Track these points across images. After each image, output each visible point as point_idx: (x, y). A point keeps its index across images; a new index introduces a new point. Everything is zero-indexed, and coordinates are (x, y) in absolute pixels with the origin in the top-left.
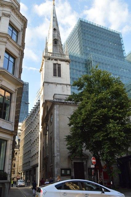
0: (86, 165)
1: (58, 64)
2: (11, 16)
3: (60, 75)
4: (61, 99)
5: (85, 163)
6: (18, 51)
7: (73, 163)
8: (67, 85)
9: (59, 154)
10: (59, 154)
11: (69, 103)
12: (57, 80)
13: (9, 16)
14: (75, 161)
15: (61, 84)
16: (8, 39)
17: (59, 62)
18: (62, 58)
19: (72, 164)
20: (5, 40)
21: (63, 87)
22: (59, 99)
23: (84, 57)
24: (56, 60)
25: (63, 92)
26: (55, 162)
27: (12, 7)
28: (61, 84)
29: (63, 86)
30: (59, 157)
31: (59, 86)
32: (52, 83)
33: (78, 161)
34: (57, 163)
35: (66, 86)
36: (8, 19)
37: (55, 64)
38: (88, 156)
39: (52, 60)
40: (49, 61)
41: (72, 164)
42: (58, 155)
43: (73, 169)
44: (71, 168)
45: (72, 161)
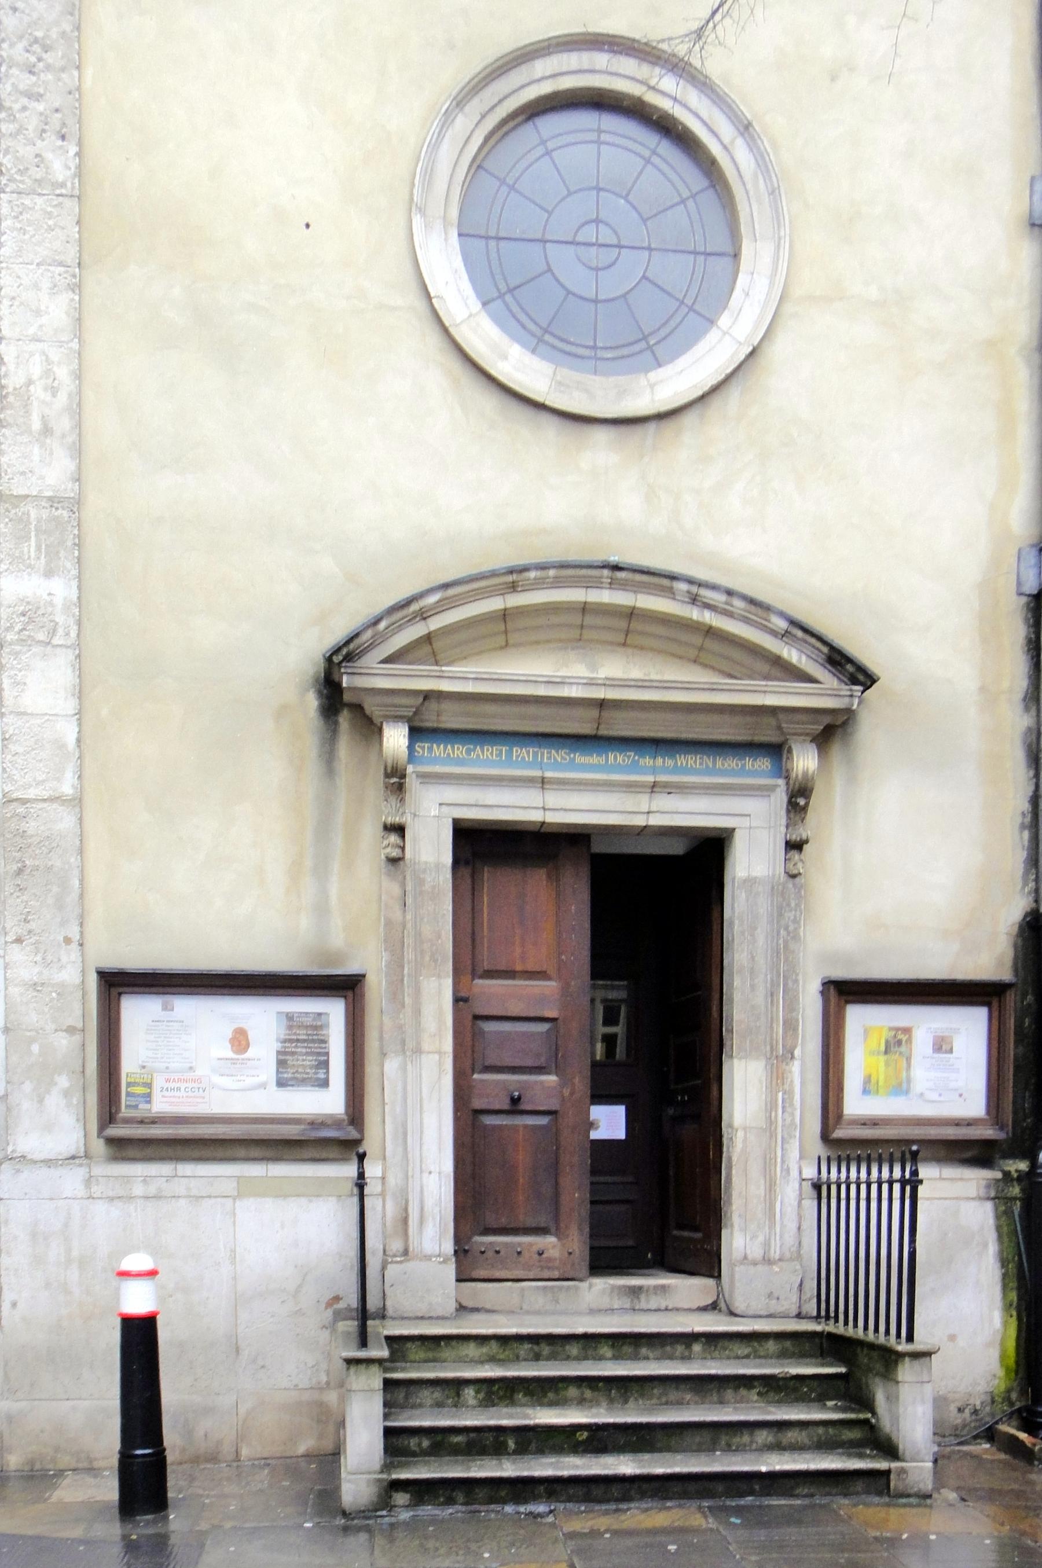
7: (433, 849)
9: (60, 590)
10: (60, 590)
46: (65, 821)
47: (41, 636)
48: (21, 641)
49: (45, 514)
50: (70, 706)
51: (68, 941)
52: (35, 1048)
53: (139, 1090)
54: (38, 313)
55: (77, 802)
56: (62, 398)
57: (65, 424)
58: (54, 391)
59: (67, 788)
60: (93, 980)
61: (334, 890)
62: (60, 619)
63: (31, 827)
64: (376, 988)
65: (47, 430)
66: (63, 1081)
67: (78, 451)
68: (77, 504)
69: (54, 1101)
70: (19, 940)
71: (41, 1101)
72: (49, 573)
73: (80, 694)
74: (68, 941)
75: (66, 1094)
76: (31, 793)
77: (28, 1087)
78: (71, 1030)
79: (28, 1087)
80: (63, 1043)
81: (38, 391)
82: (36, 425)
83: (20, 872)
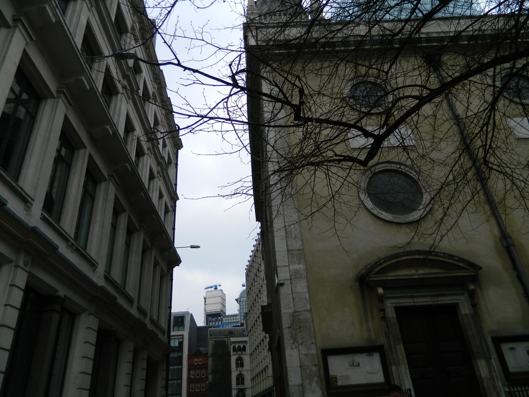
0: (476, 315)
5: (465, 310)
9: (302, 267)
10: (302, 267)
19: (384, 318)
26: (283, 311)
30: (301, 287)
33: (421, 301)
34: (294, 315)
38: (476, 267)
41: (384, 318)
42: (295, 276)
43: (400, 349)
44: (382, 341)
45: (381, 299)
46: (308, 315)
47: (299, 276)
48: (295, 278)
49: (297, 253)
50: (306, 290)
51: (312, 343)
52: (308, 371)
53: (334, 379)
54: (292, 217)
55: (310, 310)
56: (298, 231)
57: (299, 236)
58: (296, 230)
59: (308, 308)
60: (319, 352)
61: (370, 325)
62: (302, 272)
63: (301, 317)
64: (386, 347)
65: (296, 237)
66: (316, 379)
67: (302, 240)
68: (303, 250)
69: (314, 384)
70: (301, 344)
71: (311, 384)
72: (299, 264)
73: (308, 287)
74: (312, 343)
75: (317, 382)
76: (301, 310)
77: (307, 381)
78: (316, 365)
79: (307, 381)
80: (314, 369)
81: (293, 230)
82: (293, 236)
83: (300, 328)
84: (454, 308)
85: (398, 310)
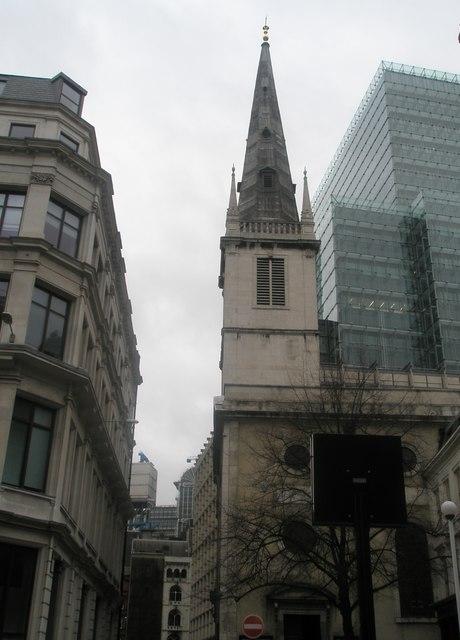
1: (273, 259)
2: (58, 177)
3: (280, 300)
4: (246, 402)
5: (323, 619)
6: (77, 279)
7: (281, 618)
8: (304, 333)
11: (271, 413)
12: (271, 318)
13: (47, 180)
14: (291, 612)
15: (282, 332)
16: (43, 253)
17: (278, 253)
18: (291, 237)
19: (276, 621)
20: (35, 257)
21: (291, 341)
22: (239, 402)
23: (402, 211)
24: (266, 245)
25: (294, 358)
27: (57, 151)
28: (282, 332)
29: (291, 337)
31: (278, 341)
32: (251, 331)
33: (300, 612)
35: (301, 338)
36: (47, 190)
37: (262, 263)
39: (252, 245)
40: (242, 251)
41: (276, 621)
45: (276, 610)
84: (318, 617)
85: (286, 616)
